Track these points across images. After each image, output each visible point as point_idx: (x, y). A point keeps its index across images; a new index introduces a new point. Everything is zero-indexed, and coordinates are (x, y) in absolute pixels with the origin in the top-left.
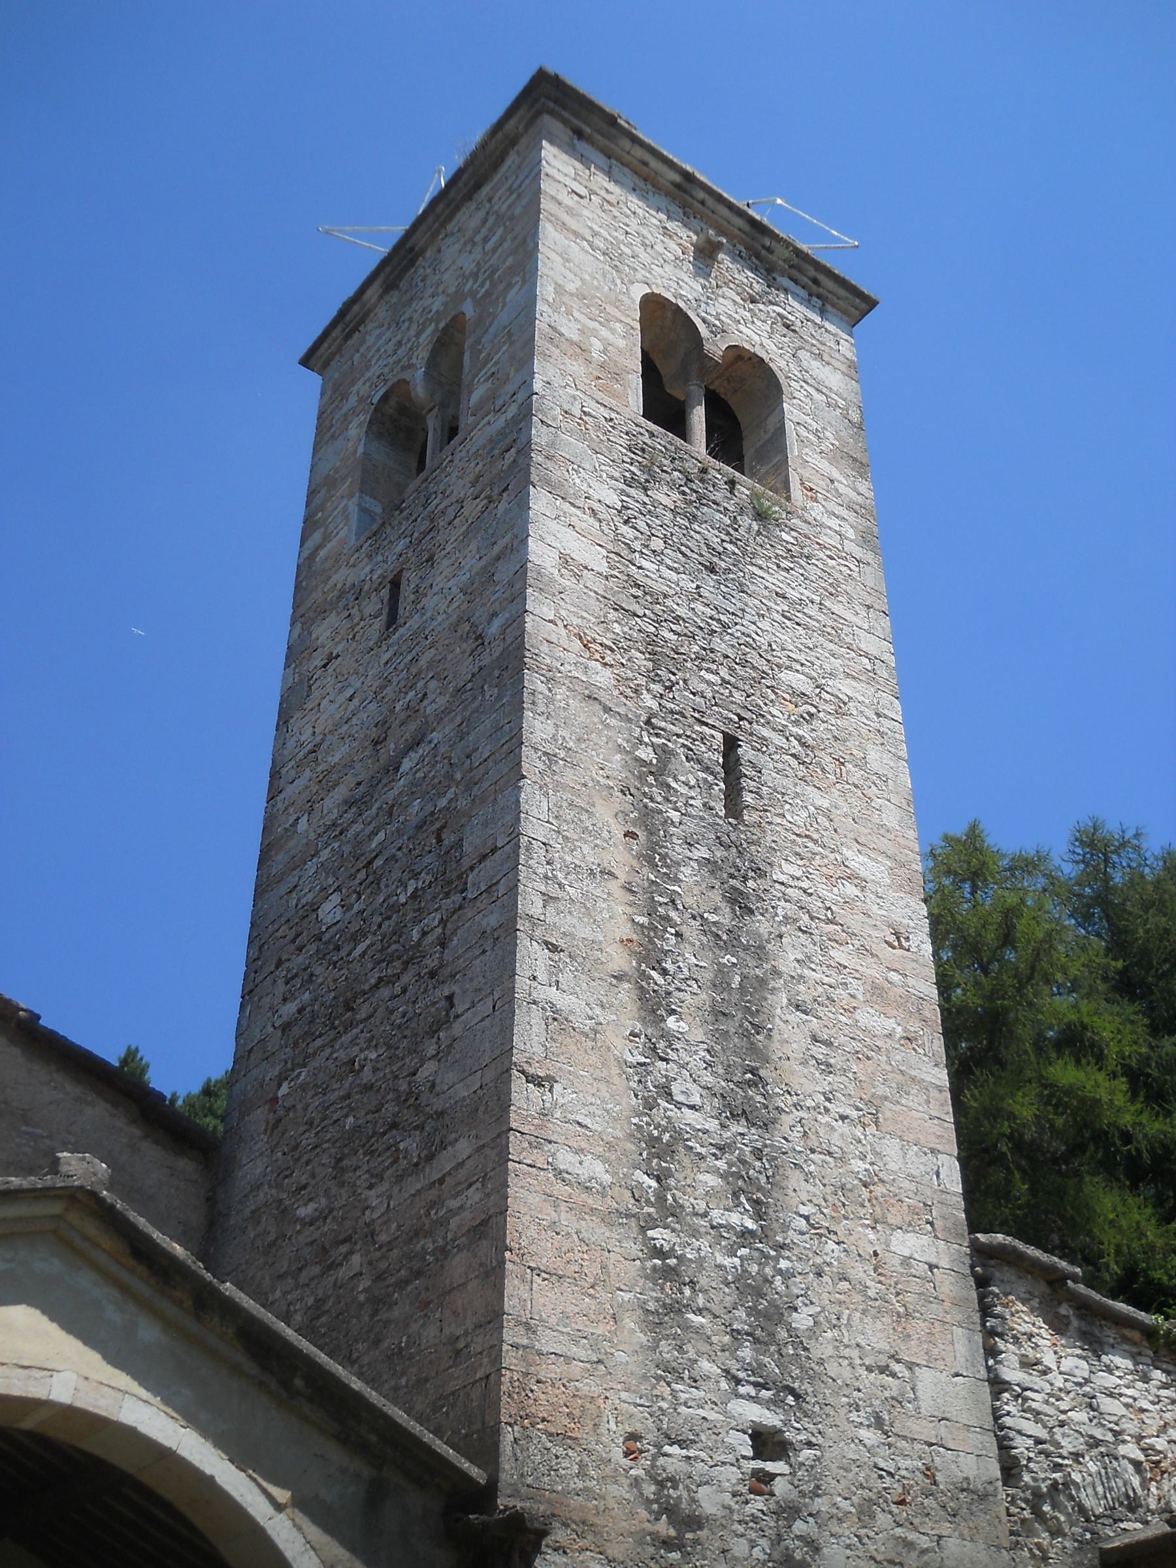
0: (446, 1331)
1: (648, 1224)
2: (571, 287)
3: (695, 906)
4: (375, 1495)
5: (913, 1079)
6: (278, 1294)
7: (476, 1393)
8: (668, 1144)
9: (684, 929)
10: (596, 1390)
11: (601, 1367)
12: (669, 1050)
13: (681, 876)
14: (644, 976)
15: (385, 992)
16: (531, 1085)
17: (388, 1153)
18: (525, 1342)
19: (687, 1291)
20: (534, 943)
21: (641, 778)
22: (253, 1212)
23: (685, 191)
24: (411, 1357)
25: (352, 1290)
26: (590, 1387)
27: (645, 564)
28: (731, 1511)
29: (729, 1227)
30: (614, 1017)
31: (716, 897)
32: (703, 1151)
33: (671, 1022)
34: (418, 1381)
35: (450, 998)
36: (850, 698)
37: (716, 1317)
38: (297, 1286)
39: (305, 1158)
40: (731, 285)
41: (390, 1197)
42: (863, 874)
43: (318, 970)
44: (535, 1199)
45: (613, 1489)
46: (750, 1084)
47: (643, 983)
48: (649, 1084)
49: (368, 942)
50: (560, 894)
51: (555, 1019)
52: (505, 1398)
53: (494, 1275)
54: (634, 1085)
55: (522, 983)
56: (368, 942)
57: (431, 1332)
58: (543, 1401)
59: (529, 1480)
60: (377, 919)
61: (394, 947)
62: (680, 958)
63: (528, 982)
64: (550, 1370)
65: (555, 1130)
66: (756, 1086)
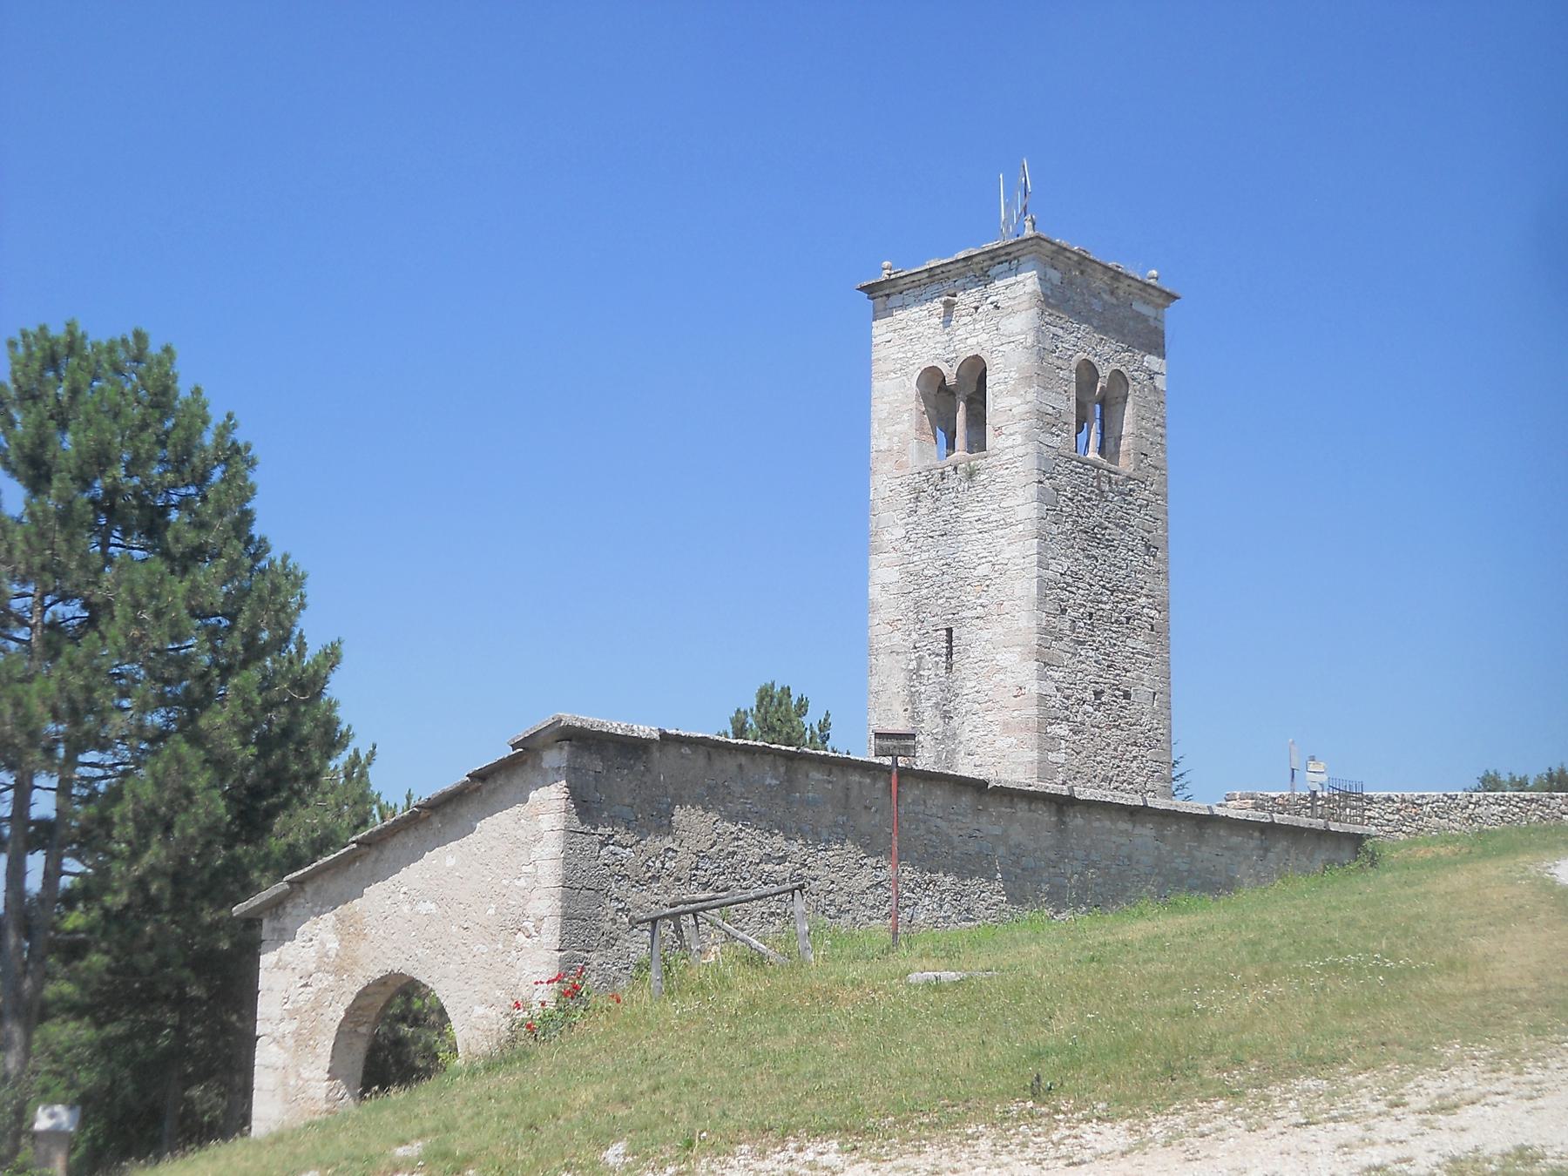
5: (1019, 764)
21: (911, 680)
27: (915, 559)
40: (964, 313)
42: (1004, 665)
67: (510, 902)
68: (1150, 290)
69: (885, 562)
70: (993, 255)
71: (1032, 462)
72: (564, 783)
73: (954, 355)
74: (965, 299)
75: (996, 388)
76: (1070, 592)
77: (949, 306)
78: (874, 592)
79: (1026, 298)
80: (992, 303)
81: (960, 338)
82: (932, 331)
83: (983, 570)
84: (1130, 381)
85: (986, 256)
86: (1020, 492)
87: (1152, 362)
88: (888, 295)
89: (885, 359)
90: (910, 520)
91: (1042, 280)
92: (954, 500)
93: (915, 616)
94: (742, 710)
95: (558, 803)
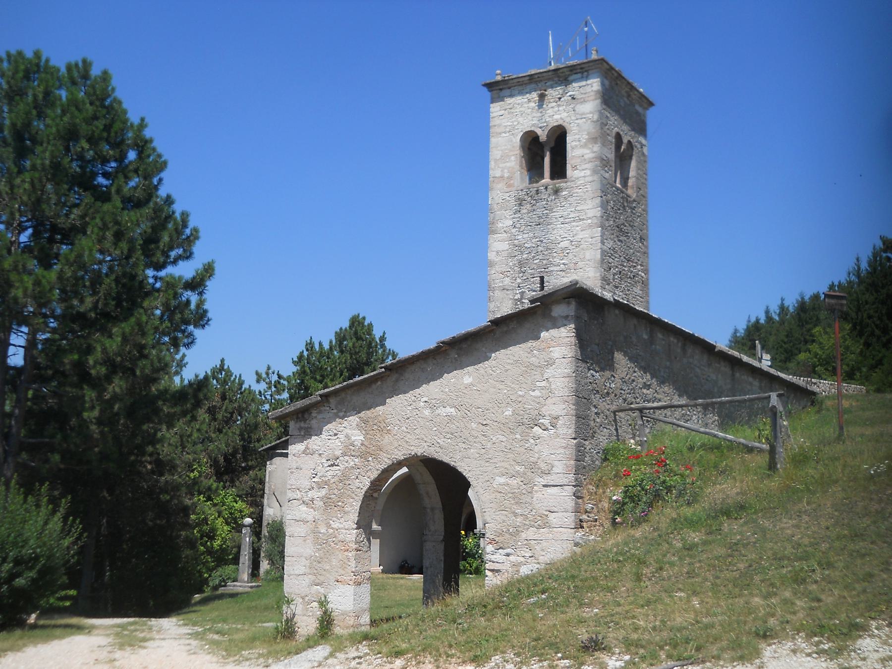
2: (498, 157)
23: (532, 79)
27: (519, 237)
36: (582, 239)
40: (552, 100)
67: (526, 406)
68: (644, 99)
69: (499, 239)
70: (573, 69)
71: (597, 185)
72: (573, 326)
73: (545, 124)
74: (553, 93)
75: (574, 143)
76: (613, 259)
77: (542, 97)
78: (492, 256)
79: (593, 93)
80: (570, 96)
81: (549, 115)
82: (530, 110)
83: (563, 244)
84: (634, 148)
85: (568, 69)
86: (589, 202)
87: (642, 139)
88: (501, 90)
89: (499, 125)
90: (516, 216)
91: (603, 84)
92: (545, 206)
93: (519, 269)
94: (344, 328)
95: (569, 339)
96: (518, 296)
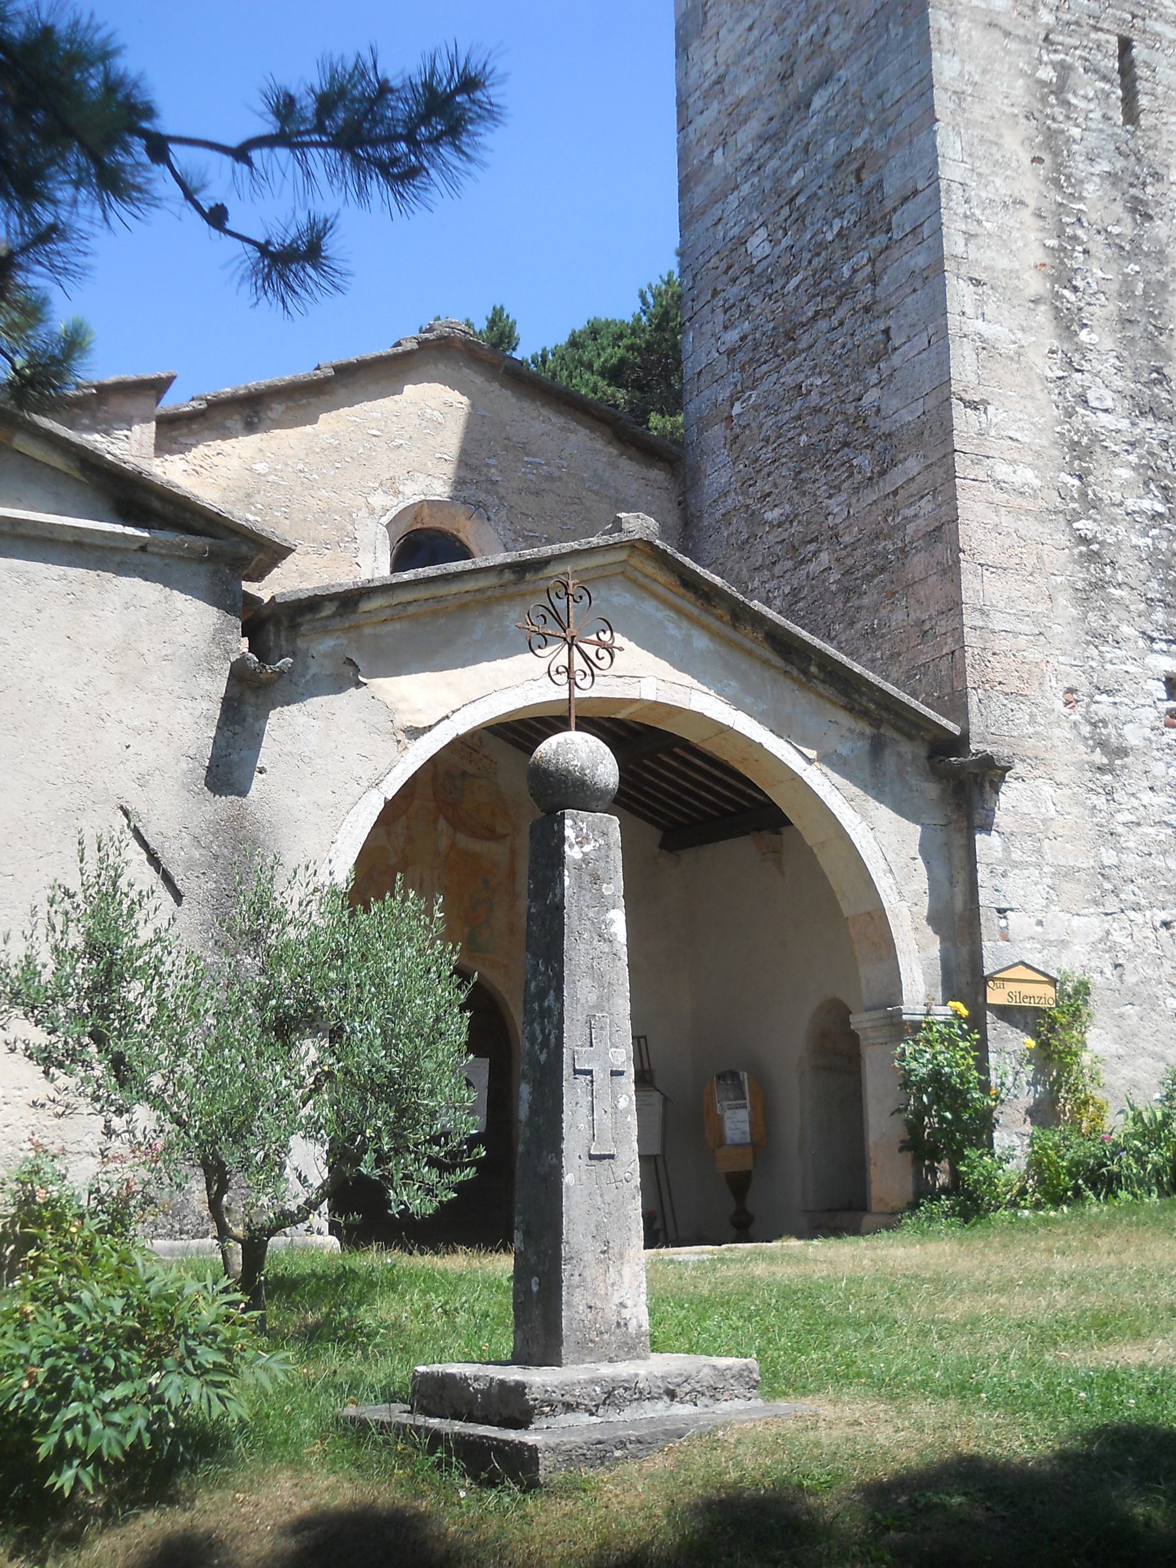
0: (913, 616)
1: (1076, 516)
3: (1099, 221)
4: (877, 747)
6: (756, 583)
7: (944, 664)
8: (1087, 447)
9: (1091, 246)
10: (1039, 657)
11: (1042, 638)
12: (1083, 362)
13: (1085, 194)
14: (1058, 296)
15: (823, 325)
16: (968, 410)
17: (844, 469)
18: (981, 624)
19: (1108, 570)
20: (961, 281)
21: (1043, 100)
22: (723, 515)
24: (883, 636)
25: (824, 581)
26: (1033, 655)
28: (1149, 740)
29: (1142, 512)
30: (1034, 339)
31: (1118, 208)
32: (1116, 448)
33: (1084, 336)
34: (892, 655)
35: (887, 331)
37: (1133, 589)
38: (773, 577)
39: (766, 470)
41: (849, 506)
43: (755, 301)
44: (979, 508)
45: (1057, 732)
46: (1155, 382)
47: (1058, 304)
48: (1068, 395)
49: (800, 277)
50: (979, 230)
51: (984, 348)
52: (969, 669)
53: (951, 572)
54: (1055, 397)
55: (953, 320)
56: (800, 277)
57: (899, 617)
58: (998, 668)
59: (993, 730)
60: (806, 256)
61: (826, 282)
62: (1088, 274)
63: (958, 318)
64: (1001, 644)
65: (992, 446)
66: (1161, 383)
96: (1047, 74)
